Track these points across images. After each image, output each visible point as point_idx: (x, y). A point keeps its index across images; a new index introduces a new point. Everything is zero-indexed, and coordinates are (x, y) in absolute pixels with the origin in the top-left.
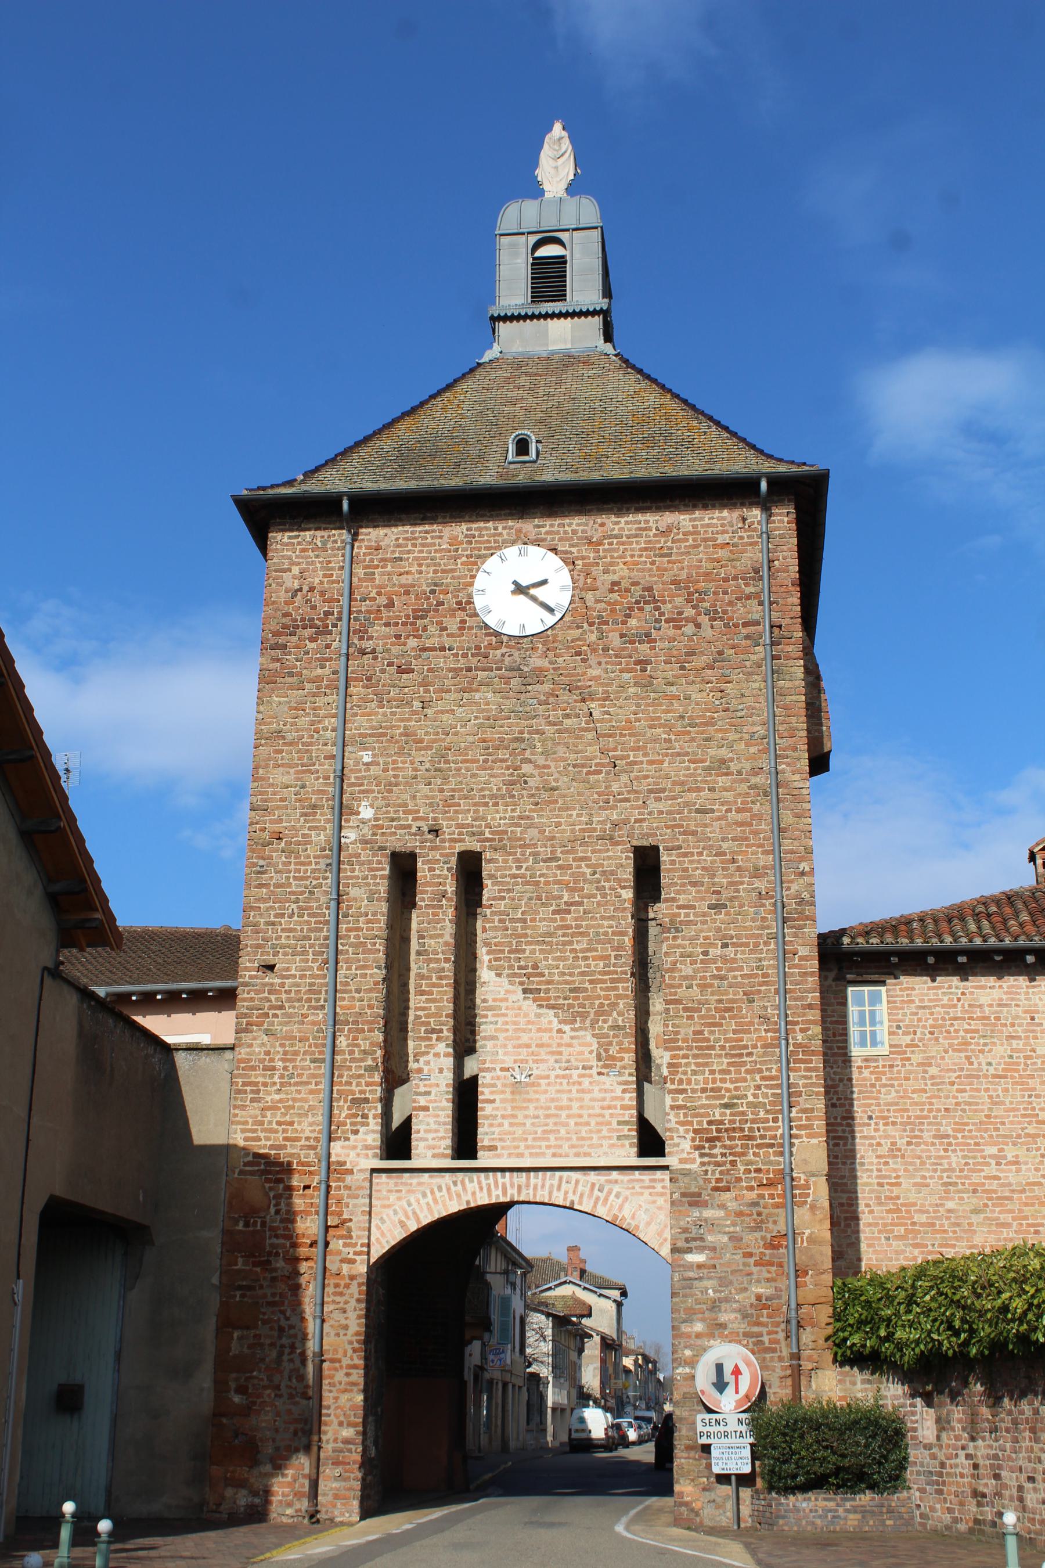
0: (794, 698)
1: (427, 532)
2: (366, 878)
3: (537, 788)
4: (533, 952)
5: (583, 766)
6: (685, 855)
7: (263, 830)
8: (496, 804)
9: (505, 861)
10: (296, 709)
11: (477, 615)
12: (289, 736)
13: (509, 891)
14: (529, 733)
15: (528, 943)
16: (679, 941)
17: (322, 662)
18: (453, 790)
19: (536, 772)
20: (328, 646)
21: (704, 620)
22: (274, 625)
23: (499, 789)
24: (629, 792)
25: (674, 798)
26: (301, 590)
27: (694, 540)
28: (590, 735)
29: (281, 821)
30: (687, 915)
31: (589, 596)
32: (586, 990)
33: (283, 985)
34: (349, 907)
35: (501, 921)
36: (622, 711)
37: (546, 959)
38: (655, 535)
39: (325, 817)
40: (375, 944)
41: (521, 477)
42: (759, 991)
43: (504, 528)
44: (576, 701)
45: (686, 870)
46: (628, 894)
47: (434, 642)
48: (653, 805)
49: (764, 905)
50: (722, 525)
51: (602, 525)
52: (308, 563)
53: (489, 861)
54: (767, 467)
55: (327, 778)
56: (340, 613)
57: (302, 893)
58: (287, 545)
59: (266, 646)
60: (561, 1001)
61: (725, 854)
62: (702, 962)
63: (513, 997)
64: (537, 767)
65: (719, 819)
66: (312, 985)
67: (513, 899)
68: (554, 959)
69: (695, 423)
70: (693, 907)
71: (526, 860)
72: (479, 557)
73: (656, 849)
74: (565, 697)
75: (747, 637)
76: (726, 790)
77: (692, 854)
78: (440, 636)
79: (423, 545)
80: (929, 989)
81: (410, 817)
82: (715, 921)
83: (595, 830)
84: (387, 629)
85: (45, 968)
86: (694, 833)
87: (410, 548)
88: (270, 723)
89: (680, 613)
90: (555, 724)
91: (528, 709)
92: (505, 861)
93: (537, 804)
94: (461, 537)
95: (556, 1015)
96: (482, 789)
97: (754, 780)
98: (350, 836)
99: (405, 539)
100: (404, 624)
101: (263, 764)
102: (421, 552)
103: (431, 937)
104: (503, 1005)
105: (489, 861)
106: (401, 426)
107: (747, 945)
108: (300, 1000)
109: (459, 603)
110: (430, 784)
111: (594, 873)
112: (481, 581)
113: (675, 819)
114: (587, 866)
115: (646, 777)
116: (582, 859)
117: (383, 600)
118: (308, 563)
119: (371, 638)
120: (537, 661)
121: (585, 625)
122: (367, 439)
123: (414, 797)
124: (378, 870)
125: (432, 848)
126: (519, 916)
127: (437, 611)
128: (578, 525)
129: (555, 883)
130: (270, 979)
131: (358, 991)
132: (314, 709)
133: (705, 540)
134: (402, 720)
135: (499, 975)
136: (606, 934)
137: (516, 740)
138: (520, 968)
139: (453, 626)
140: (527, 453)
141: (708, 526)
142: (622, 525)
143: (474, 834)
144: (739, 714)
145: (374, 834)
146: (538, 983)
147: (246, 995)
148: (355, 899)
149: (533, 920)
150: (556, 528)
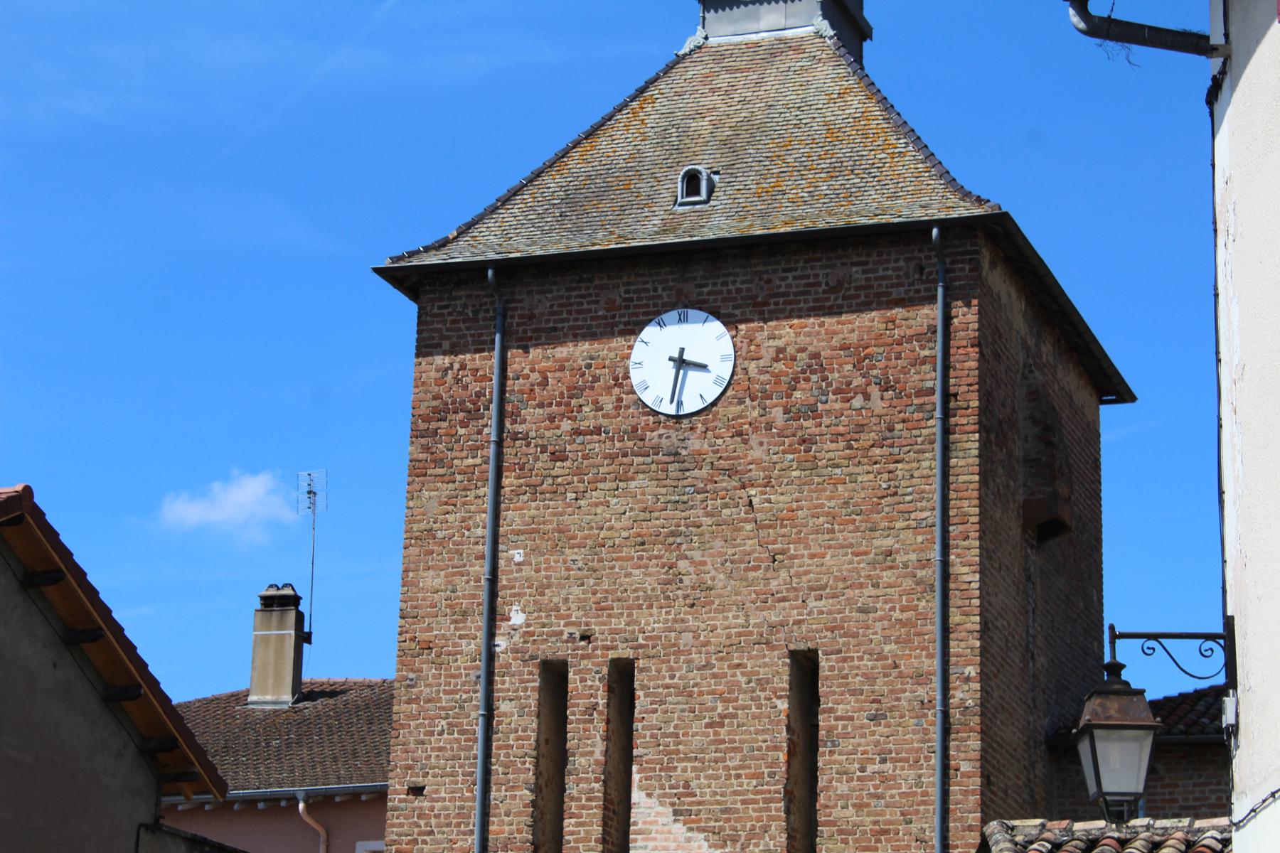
0: (966, 478)
1: (582, 296)
2: (517, 690)
3: (693, 588)
4: (684, 770)
5: (741, 562)
6: (845, 660)
7: (413, 639)
8: (650, 607)
9: (659, 671)
10: (446, 504)
11: (634, 393)
12: (440, 534)
13: (662, 703)
14: (687, 526)
15: (681, 760)
16: (836, 757)
17: (474, 450)
18: (607, 592)
19: (692, 569)
20: (480, 432)
21: (875, 391)
22: (423, 410)
23: (653, 589)
24: (788, 590)
25: (834, 596)
26: (451, 367)
27: (866, 296)
28: (749, 527)
29: (430, 629)
30: (845, 727)
31: (752, 367)
32: (737, 811)
33: (432, 809)
34: (500, 723)
35: (652, 736)
36: (781, 500)
37: (698, 778)
38: (824, 292)
39: (478, 623)
40: (524, 763)
42: (917, 812)
43: (664, 289)
44: (735, 488)
45: (846, 677)
46: (783, 705)
47: (592, 424)
48: (812, 603)
49: (925, 715)
50: (898, 277)
53: (642, 670)
55: (478, 580)
56: (491, 393)
57: (452, 708)
59: (416, 434)
60: (712, 824)
61: (886, 658)
62: (859, 779)
63: (662, 820)
64: (693, 562)
65: (881, 619)
66: (462, 808)
67: (666, 712)
68: (707, 777)
70: (851, 719)
71: (680, 669)
73: (815, 652)
74: (725, 483)
75: (920, 408)
76: (890, 586)
77: (852, 658)
78: (595, 417)
79: (578, 312)
80: (1195, 785)
81: (562, 622)
82: (873, 733)
83: (751, 633)
84: (541, 411)
85: (141, 826)
86: (855, 635)
87: (565, 315)
88: (420, 521)
89: (849, 384)
90: (713, 516)
91: (685, 498)
92: (659, 671)
93: (693, 605)
94: (619, 302)
95: (706, 840)
96: (635, 591)
97: (921, 573)
98: (501, 643)
99: (560, 305)
100: (559, 404)
101: (412, 566)
102: (576, 320)
103: (583, 755)
104: (654, 828)
105: (642, 670)
106: (575, 154)
107: (907, 760)
108: (449, 825)
109: (616, 379)
110: (582, 585)
111: (749, 682)
113: (835, 619)
114: (743, 674)
115: (806, 573)
116: (738, 666)
117: (536, 377)
118: (459, 337)
120: (695, 444)
121: (748, 400)
122: (516, 192)
123: (566, 600)
124: (528, 681)
125: (583, 657)
126: (672, 730)
127: (592, 388)
128: (743, 282)
129: (709, 693)
130: (418, 802)
131: (507, 815)
133: (879, 295)
134: (555, 515)
135: (649, 795)
136: (760, 749)
137: (673, 534)
138: (671, 787)
139: (609, 407)
140: (698, 193)
141: (883, 278)
142: (790, 281)
143: (627, 641)
144: (908, 498)
145: (525, 642)
146: (689, 804)
147: (395, 821)
148: (505, 715)
149: (685, 734)
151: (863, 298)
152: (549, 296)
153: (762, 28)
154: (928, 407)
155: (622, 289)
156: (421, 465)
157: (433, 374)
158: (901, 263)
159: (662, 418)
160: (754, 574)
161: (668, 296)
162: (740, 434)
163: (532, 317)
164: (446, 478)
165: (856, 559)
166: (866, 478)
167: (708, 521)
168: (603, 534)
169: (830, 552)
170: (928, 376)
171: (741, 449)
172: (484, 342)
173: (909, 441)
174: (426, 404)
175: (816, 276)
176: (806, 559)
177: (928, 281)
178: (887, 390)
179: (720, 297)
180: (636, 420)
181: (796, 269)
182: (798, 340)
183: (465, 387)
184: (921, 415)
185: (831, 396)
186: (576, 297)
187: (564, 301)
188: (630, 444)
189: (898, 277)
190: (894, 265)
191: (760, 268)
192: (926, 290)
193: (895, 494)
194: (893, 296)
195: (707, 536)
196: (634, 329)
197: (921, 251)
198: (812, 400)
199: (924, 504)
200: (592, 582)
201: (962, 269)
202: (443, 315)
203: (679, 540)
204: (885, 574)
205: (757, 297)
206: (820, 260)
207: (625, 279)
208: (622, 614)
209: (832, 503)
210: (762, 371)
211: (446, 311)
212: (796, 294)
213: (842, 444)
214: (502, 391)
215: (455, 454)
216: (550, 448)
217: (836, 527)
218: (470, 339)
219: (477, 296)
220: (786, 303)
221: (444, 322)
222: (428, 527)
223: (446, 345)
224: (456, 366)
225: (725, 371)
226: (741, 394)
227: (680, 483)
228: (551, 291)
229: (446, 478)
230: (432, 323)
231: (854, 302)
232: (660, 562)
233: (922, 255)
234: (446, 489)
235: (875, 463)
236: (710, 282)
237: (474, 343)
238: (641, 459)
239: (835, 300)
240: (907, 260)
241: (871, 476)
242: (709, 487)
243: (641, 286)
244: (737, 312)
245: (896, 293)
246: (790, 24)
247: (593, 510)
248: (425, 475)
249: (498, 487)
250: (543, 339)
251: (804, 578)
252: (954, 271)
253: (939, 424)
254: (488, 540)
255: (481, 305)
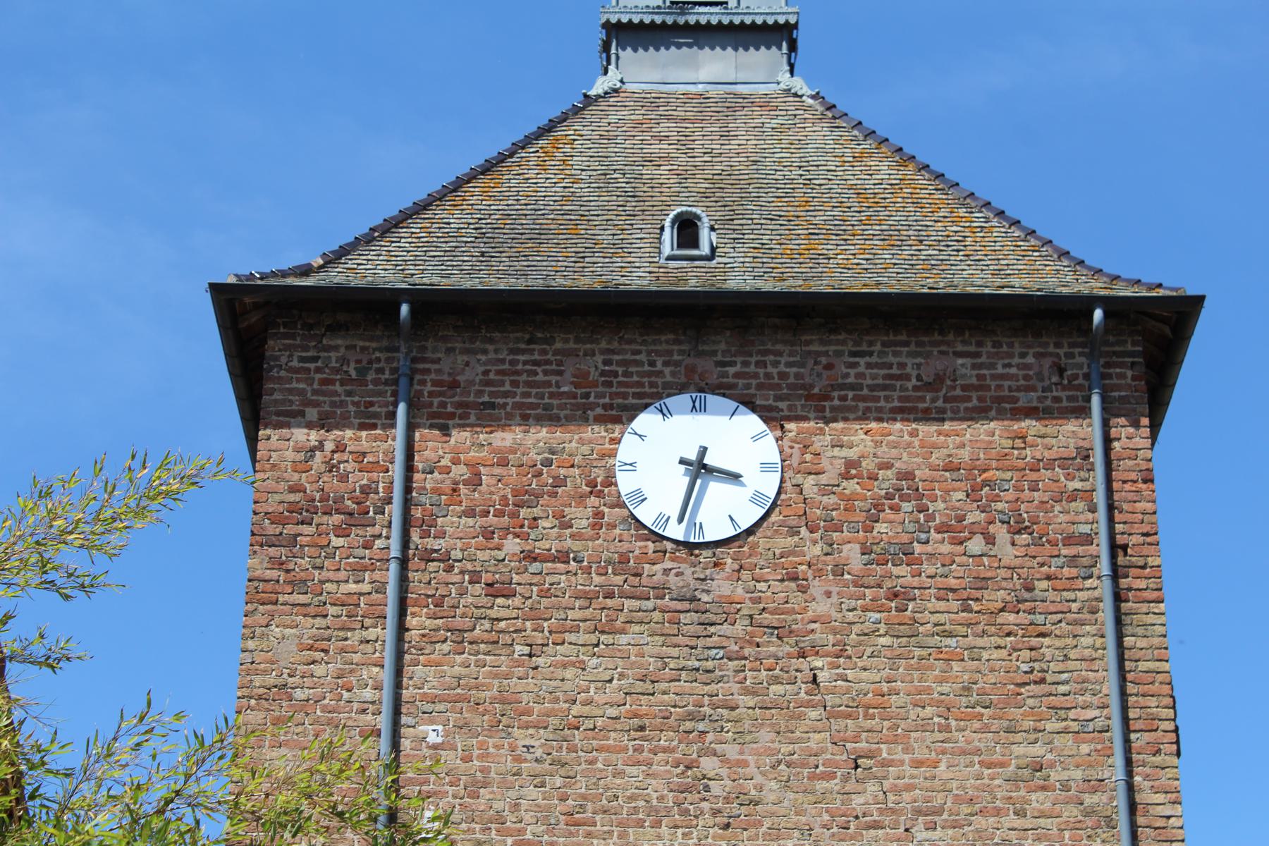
3: (727, 800)
5: (803, 766)
8: (657, 824)
11: (622, 505)
12: (299, 694)
14: (715, 707)
17: (358, 571)
18: (584, 797)
19: (724, 772)
20: (368, 546)
21: (1001, 532)
22: (273, 504)
23: (661, 798)
26: (321, 446)
27: (980, 399)
28: (814, 714)
36: (865, 676)
38: (916, 388)
41: (693, 279)
43: (666, 364)
47: (555, 546)
51: (829, 367)
52: (333, 404)
54: (1097, 287)
56: (389, 489)
58: (297, 371)
59: (260, 540)
69: (962, 212)
72: (625, 408)
75: (1073, 560)
76: (1042, 815)
78: (560, 537)
79: (529, 384)
84: (471, 521)
88: (265, 672)
89: (961, 519)
90: (755, 694)
91: (710, 665)
93: (727, 826)
96: (632, 798)
97: (1089, 800)
99: (498, 372)
100: (499, 514)
102: (527, 395)
106: (475, 188)
110: (543, 785)
112: (628, 448)
118: (333, 404)
119: (442, 535)
120: (722, 586)
121: (803, 530)
123: (516, 807)
128: (789, 365)
132: (343, 650)
134: (496, 676)
140: (696, 245)
141: (1003, 377)
142: (862, 369)
150: (752, 368)
151: (975, 402)
152: (483, 358)
153: (702, 78)
154: (1085, 561)
155: (599, 359)
156: (269, 587)
157: (290, 455)
158: (1030, 360)
159: (669, 546)
160: (825, 784)
161: (673, 374)
162: (794, 578)
163: (454, 385)
164: (312, 610)
165: (987, 772)
166: (996, 654)
167: (750, 701)
168: (575, 710)
169: (944, 758)
170: (1082, 518)
171: (797, 600)
172: (376, 415)
173: (1059, 607)
174: (278, 497)
175: (902, 366)
176: (906, 767)
177: (1070, 387)
178: (1019, 532)
179: (754, 382)
180: (625, 547)
181: (871, 354)
182: (880, 451)
183: (344, 478)
184: (1074, 572)
185: (934, 535)
186: (525, 363)
187: (506, 366)
188: (619, 579)
189: (1026, 377)
190: (1017, 361)
191: (815, 347)
192: (1070, 399)
193: (1043, 681)
194: (1020, 404)
195: (747, 724)
196: (621, 414)
197: (1058, 345)
198: (905, 538)
199: (1088, 698)
200: (559, 781)
201: (1123, 376)
202: (309, 370)
203: (701, 726)
204: (1034, 796)
205: (812, 386)
206: (907, 344)
207: (603, 345)
208: (610, 832)
209: (945, 688)
210: (826, 490)
211: (312, 366)
212: (872, 388)
213: (955, 605)
214: (408, 489)
215: (325, 575)
216: (486, 577)
217: (953, 723)
218: (352, 409)
219: (363, 349)
220: (855, 398)
221: (310, 381)
222: (279, 681)
223: (312, 414)
224: (329, 446)
225: (770, 485)
226: (793, 521)
227: (701, 642)
228: (485, 352)
229: (312, 610)
230: (290, 380)
231: (962, 406)
232: (671, 758)
233: (1061, 352)
234: (310, 627)
235: (1008, 635)
236: (739, 359)
237: (358, 414)
238: (636, 604)
239: (934, 400)
240: (1038, 356)
241: (1004, 653)
242: (746, 651)
243: (628, 357)
244: (783, 405)
245: (1024, 400)
246: (741, 78)
247: (559, 673)
248: (276, 603)
249: (402, 628)
250: (472, 419)
251: (906, 796)
252: (1110, 376)
253: (1107, 583)
254: (386, 708)
255: (370, 362)
